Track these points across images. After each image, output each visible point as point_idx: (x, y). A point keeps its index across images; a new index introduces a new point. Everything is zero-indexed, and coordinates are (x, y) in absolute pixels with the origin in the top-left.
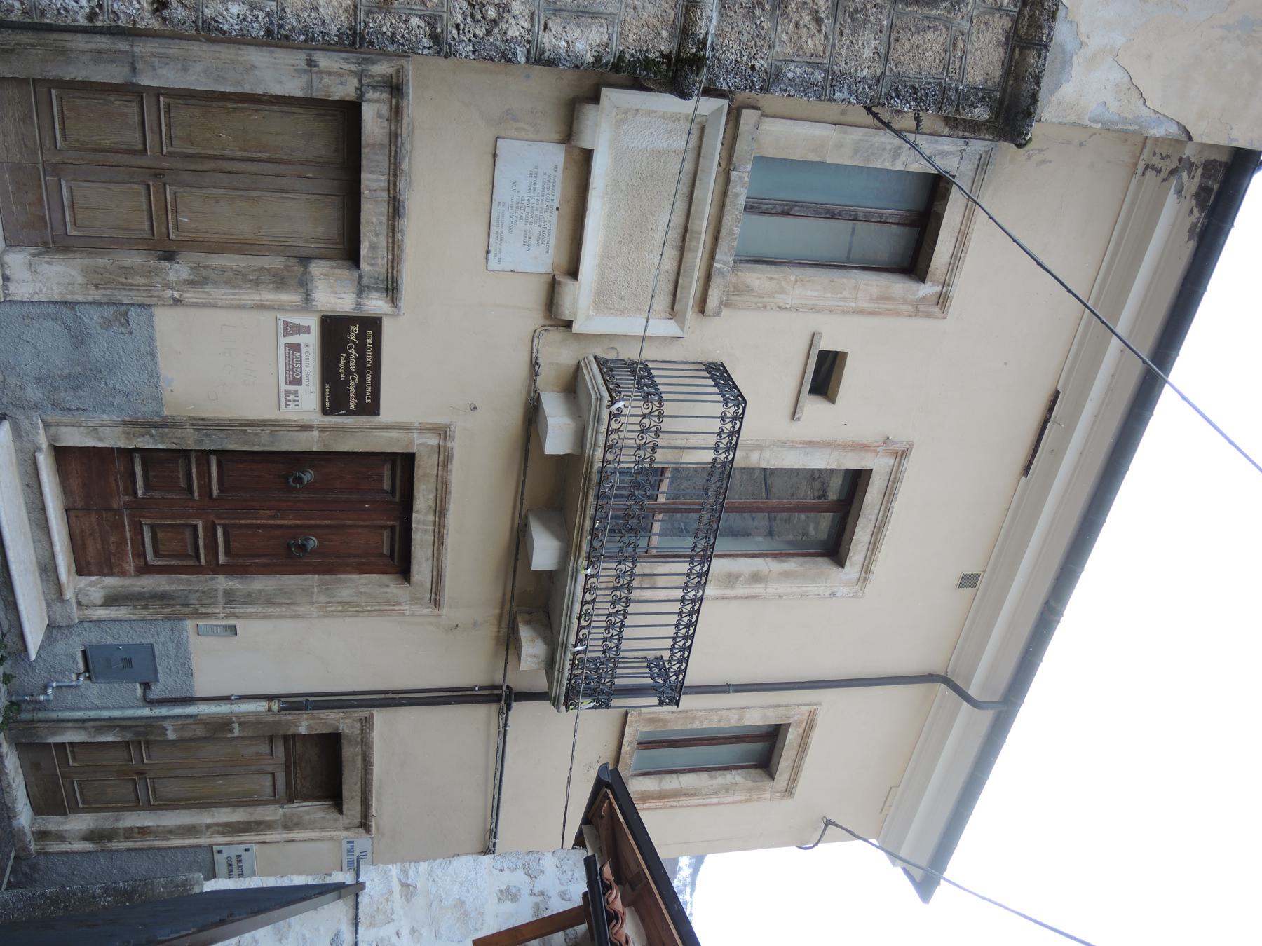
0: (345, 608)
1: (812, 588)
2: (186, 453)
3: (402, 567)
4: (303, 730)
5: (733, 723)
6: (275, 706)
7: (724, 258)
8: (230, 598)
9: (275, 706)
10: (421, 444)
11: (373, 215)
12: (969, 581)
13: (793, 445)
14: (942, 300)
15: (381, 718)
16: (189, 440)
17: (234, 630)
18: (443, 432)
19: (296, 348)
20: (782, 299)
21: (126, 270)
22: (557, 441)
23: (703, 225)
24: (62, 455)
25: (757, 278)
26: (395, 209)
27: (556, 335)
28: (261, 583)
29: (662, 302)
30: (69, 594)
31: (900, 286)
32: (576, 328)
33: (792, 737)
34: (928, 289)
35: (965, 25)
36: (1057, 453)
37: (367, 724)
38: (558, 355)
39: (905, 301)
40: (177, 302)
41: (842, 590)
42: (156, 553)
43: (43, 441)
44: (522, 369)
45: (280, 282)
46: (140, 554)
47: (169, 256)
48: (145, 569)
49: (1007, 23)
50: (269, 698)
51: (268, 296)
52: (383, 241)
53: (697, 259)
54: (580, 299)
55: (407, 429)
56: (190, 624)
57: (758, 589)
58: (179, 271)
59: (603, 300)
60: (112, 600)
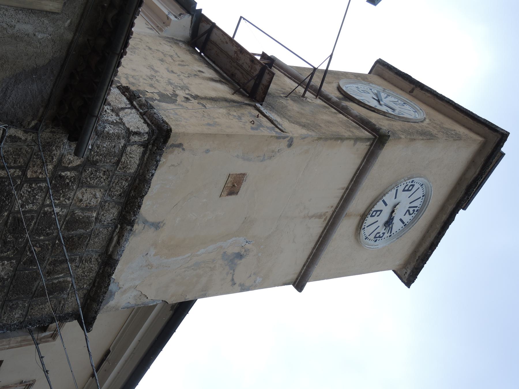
35: (65, 296)
49: (85, 291)
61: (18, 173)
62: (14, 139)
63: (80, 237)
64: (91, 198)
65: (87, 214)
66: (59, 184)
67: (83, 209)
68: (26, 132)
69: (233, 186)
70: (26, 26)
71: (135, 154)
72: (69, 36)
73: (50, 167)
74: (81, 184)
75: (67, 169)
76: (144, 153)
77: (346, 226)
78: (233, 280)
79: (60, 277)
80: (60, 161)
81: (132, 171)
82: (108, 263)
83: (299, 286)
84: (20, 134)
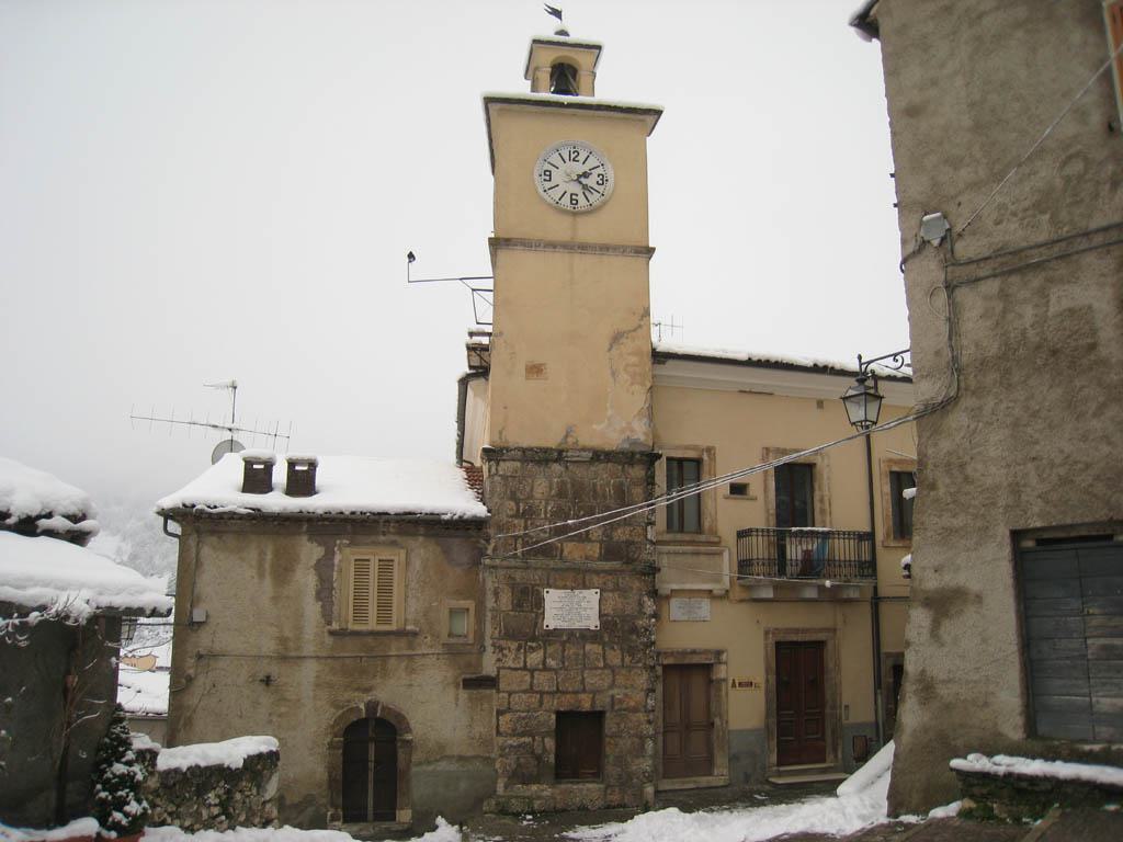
0: (838, 665)
1: (825, 477)
2: (779, 723)
3: (820, 645)
4: (891, 680)
5: (889, 497)
6: (879, 691)
7: (702, 538)
8: (834, 707)
9: (879, 691)
10: (771, 640)
11: (696, 660)
12: (820, 404)
13: (766, 497)
14: (709, 450)
15: (885, 649)
16: (773, 720)
17: (847, 707)
18: (767, 633)
19: (740, 684)
20: (713, 513)
21: (718, 737)
22: (768, 593)
23: (689, 548)
24: (780, 764)
25: (707, 524)
26: (694, 652)
27: (731, 594)
28: (828, 696)
29: (717, 557)
30: (832, 765)
31: (706, 468)
32: (728, 588)
33: (895, 469)
34: (705, 457)
36: (764, 386)
37: (889, 655)
38: (737, 593)
39: (710, 464)
40: (727, 722)
41: (826, 461)
42: (817, 733)
43: (775, 768)
44: (744, 606)
45: (719, 690)
46: (817, 739)
47: (713, 724)
48: (823, 739)
50: (876, 694)
51: (723, 693)
52: (704, 656)
53: (702, 549)
54: (717, 588)
55: (766, 646)
56: (844, 722)
57: (826, 499)
58: (717, 721)
59: (717, 580)
60: (835, 750)
61: (520, 541)
62: (495, 549)
63: (573, 486)
64: (541, 485)
65: (555, 486)
66: (528, 514)
67: (551, 489)
68: (489, 544)
69: (535, 370)
70: (417, 564)
71: (506, 467)
72: (421, 539)
73: (516, 521)
74: (531, 496)
75: (518, 510)
76: (504, 460)
77: (589, 230)
78: (635, 330)
79: (610, 490)
80: (512, 516)
81: (519, 464)
82: (599, 456)
83: (650, 251)
84: (491, 547)
